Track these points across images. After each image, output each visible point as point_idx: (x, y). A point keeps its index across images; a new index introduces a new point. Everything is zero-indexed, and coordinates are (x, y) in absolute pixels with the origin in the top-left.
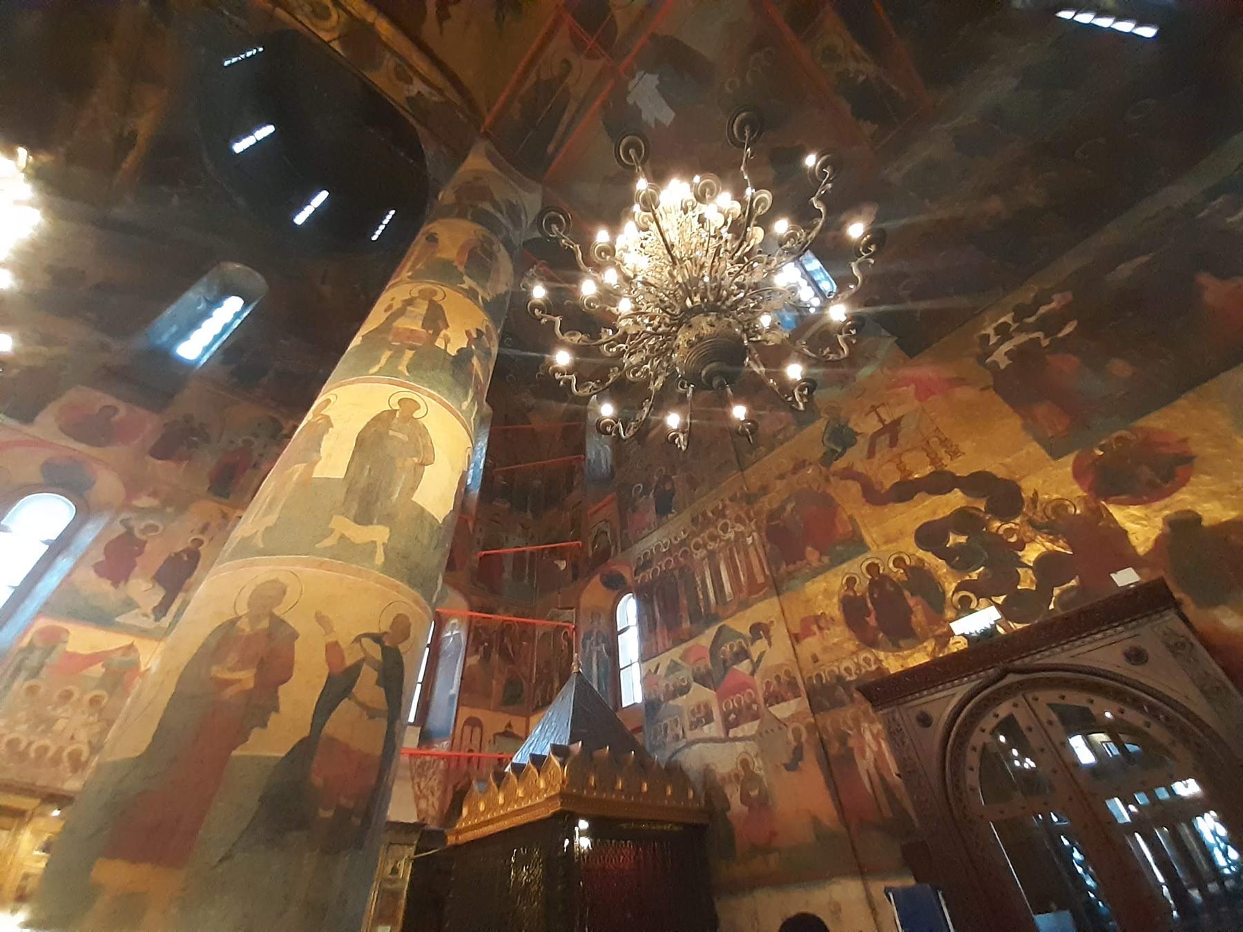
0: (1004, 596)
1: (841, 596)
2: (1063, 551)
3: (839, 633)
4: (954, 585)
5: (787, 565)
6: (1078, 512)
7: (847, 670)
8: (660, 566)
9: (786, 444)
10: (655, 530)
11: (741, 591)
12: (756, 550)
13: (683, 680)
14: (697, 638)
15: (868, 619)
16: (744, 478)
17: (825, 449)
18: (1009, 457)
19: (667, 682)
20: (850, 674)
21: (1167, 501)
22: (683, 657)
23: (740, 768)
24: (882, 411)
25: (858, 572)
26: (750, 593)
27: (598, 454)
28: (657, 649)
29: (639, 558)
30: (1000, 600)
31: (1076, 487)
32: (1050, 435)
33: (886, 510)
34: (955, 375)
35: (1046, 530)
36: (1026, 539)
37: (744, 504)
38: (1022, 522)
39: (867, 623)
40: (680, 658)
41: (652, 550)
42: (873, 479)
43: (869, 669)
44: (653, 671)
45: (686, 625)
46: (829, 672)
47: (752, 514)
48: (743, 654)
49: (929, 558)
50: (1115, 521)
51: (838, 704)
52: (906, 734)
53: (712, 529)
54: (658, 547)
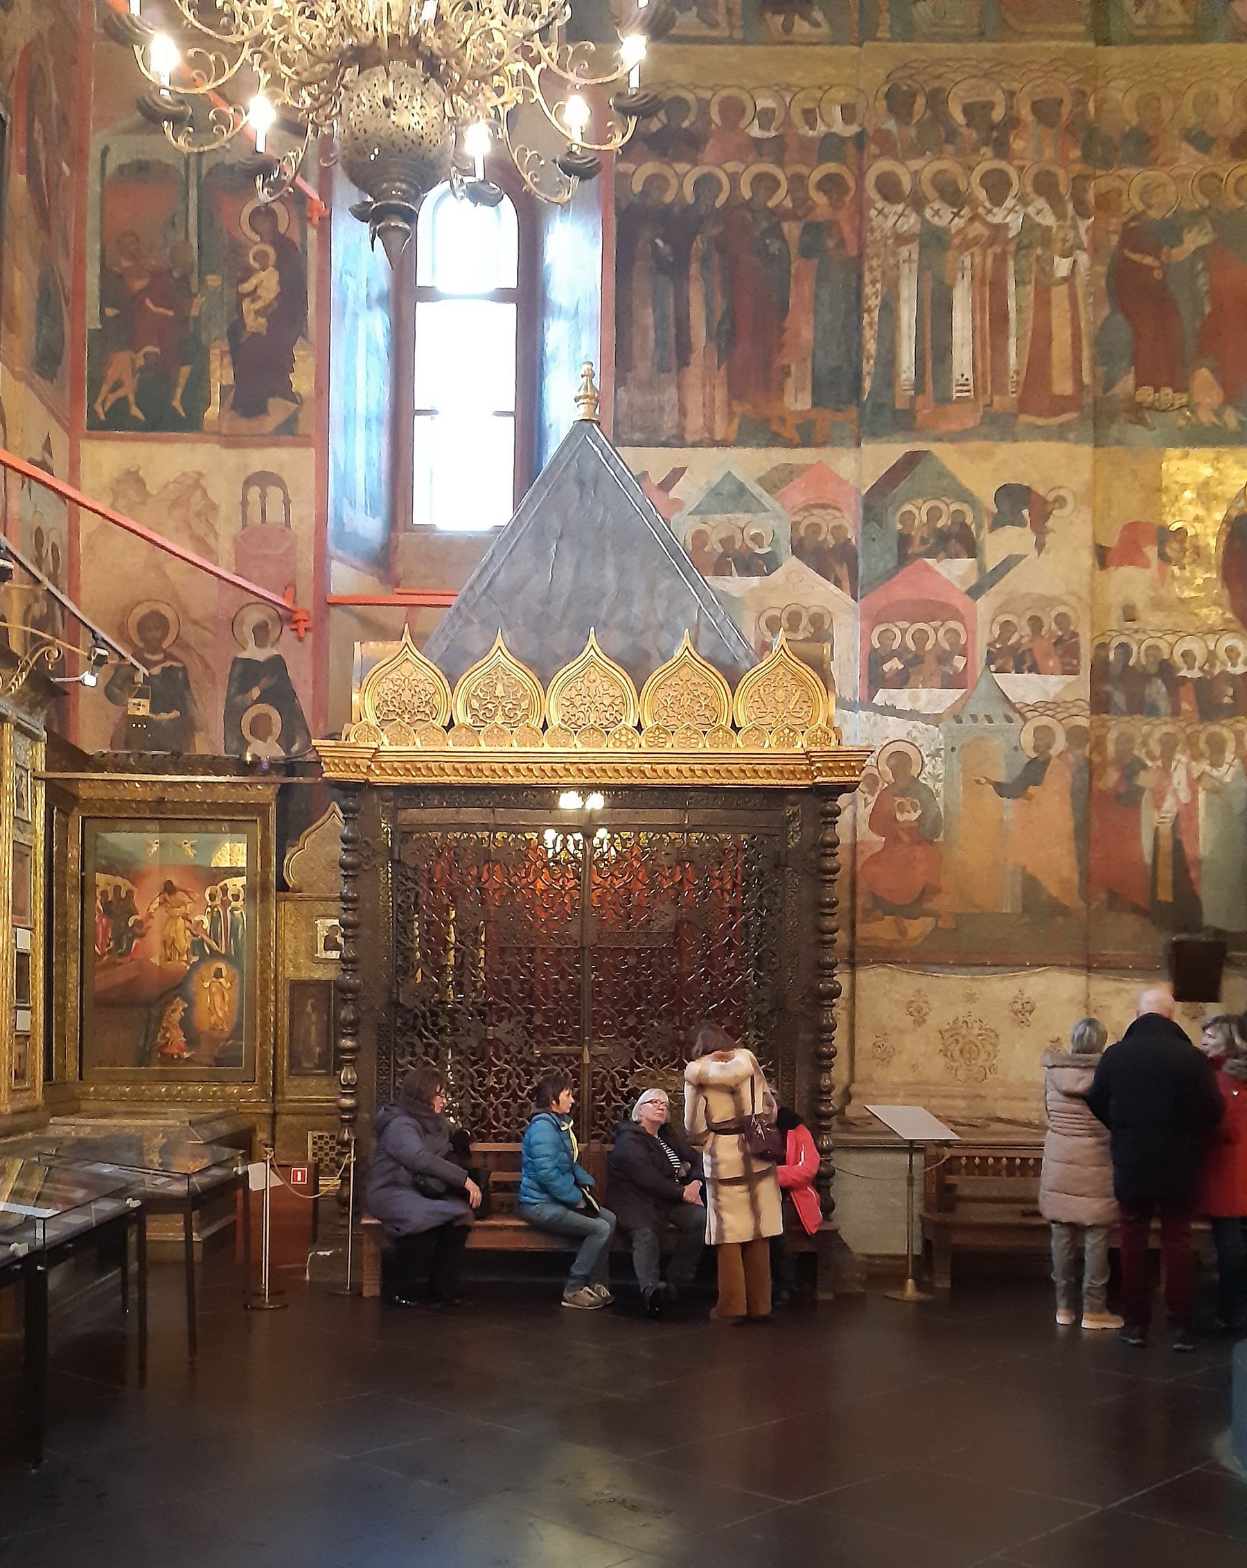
1: (1234, 513)
3: (1199, 581)
5: (1138, 385)
8: (734, 179)
13: (757, 539)
19: (704, 527)
20: (1190, 668)
26: (1023, 406)
28: (681, 427)
37: (1076, 153)
40: (760, 481)
41: (704, 105)
43: (1230, 669)
44: (656, 478)
46: (1149, 647)
47: (1091, 196)
51: (1140, 707)
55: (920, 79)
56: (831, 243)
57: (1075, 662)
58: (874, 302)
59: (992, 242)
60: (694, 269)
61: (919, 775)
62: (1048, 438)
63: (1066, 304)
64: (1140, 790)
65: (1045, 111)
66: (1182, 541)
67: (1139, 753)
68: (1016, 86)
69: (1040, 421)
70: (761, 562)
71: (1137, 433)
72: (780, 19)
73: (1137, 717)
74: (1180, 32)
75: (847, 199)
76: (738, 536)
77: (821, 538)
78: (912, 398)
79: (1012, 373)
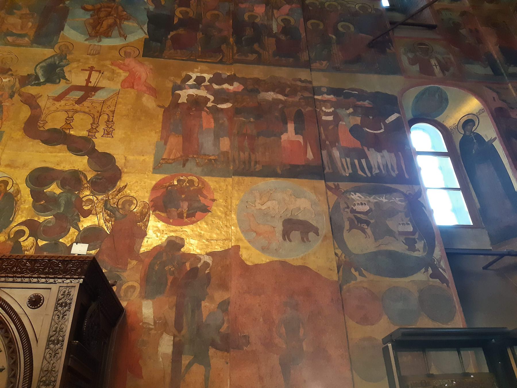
2: (106, 229)
4: (24, 219)
6: (135, 210)
17: (33, 72)
18: (134, 155)
21: (178, 228)
24: (95, 75)
30: (41, 243)
31: (148, 195)
32: (164, 157)
33: (31, 143)
34: (154, 87)
35: (109, 212)
36: (94, 212)
38: (102, 199)
42: (43, 116)
49: (26, 193)
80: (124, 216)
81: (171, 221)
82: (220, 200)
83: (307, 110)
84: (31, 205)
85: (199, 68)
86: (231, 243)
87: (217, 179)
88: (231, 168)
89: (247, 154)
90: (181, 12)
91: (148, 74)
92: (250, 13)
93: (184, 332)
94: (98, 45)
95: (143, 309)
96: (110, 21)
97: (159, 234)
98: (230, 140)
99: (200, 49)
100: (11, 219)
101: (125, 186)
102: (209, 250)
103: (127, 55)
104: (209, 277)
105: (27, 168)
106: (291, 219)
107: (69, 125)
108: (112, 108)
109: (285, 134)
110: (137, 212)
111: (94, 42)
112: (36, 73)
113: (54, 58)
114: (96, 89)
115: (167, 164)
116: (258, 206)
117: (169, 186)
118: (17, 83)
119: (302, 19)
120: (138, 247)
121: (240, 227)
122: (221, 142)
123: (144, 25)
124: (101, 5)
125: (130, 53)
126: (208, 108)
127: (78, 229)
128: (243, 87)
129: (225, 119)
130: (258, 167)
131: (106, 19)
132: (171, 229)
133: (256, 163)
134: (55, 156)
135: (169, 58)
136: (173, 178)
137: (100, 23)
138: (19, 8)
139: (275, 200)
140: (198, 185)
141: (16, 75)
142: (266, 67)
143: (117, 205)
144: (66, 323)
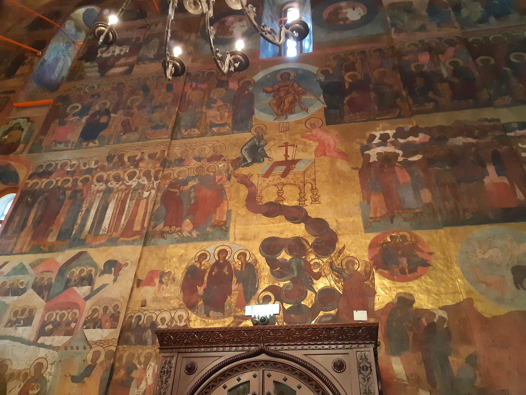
0: (291, 305)
1: (190, 265)
2: (338, 290)
6: (359, 269)
7: (163, 320)
9: (216, 138)
10: (71, 149)
11: (116, 230)
12: (147, 204)
13: (22, 284)
14: (55, 254)
15: (199, 288)
16: (170, 144)
18: (343, 218)
19: (6, 280)
20: (163, 324)
21: (404, 284)
22: (33, 265)
23: (32, 369)
24: (290, 149)
25: (212, 252)
26: (122, 235)
27: (57, 60)
28: (13, 249)
29: (41, 166)
30: (287, 306)
31: (366, 254)
32: (371, 216)
33: (255, 217)
34: (344, 151)
35: (336, 273)
36: (323, 274)
38: (327, 262)
39: (196, 290)
40: (31, 265)
41: (57, 164)
42: (259, 192)
43: (179, 324)
45: (52, 239)
46: (148, 317)
47: (160, 175)
48: (89, 280)
49: (262, 261)
50: (374, 285)
51: (141, 342)
52: (172, 376)
53: (120, 172)
54: (64, 165)
55: (118, 152)
56: (79, 195)
57: (116, 323)
58: (84, 209)
59: (125, 190)
60: (36, 205)
61: (44, 372)
62: (127, 244)
63: (144, 204)
64: (133, 379)
65: (152, 156)
66: (169, 276)
67: (135, 362)
68: (145, 151)
69: (126, 239)
70: (20, 291)
71: (161, 241)
72: (85, 143)
73: (137, 346)
74: (196, 135)
75: (88, 183)
76: (16, 283)
77: (43, 282)
78: (87, 236)
79: (121, 226)
80: (351, 276)
81: (395, 277)
82: (437, 253)
83: (503, 149)
84: (269, 272)
85: (381, 126)
86: (461, 296)
87: (428, 231)
88: (440, 218)
89: (452, 202)
90: (349, 77)
91: (336, 140)
92: (415, 64)
93: (438, 387)
94: (286, 122)
95: (393, 365)
96: (290, 98)
97: (387, 292)
98: (431, 191)
99: (376, 108)
100: (256, 287)
101: (344, 248)
102: (441, 305)
103: (313, 126)
104: (448, 331)
105: (258, 240)
106: (519, 266)
107: (281, 198)
108: (313, 177)
109: (486, 177)
110: (361, 271)
111: (282, 120)
112: (243, 155)
113: (254, 140)
114: (294, 162)
115: (376, 223)
116: (480, 256)
117: (384, 243)
118: (230, 167)
119: (470, 59)
120: (372, 305)
121: (467, 279)
122: (421, 194)
123: (320, 96)
124: (279, 86)
125: (315, 124)
126: (399, 163)
127: (314, 292)
128: (429, 137)
129: (419, 171)
130: (468, 216)
131: (286, 98)
132: (398, 286)
133: (465, 211)
134: (278, 226)
135: (351, 122)
136: (385, 235)
137: (282, 102)
138: (215, 102)
139: (496, 247)
140: (411, 240)
141: (228, 160)
142: (446, 113)
143: (342, 266)
144: (373, 385)
